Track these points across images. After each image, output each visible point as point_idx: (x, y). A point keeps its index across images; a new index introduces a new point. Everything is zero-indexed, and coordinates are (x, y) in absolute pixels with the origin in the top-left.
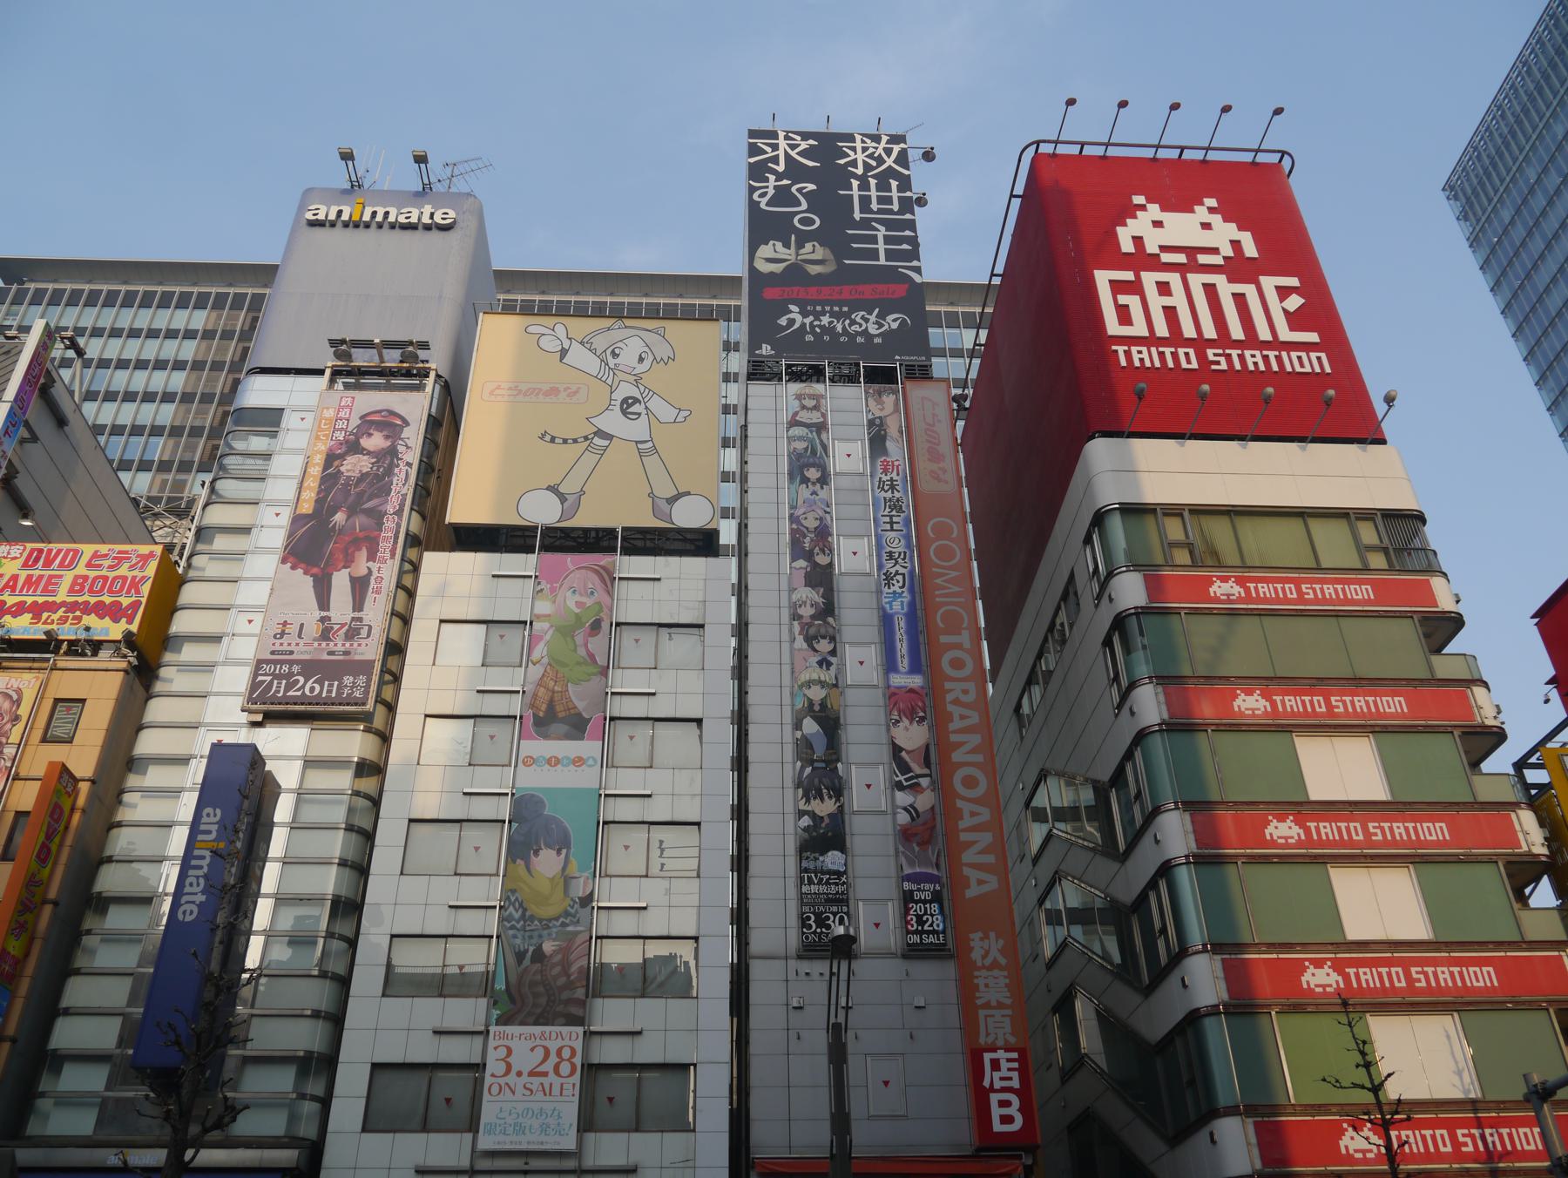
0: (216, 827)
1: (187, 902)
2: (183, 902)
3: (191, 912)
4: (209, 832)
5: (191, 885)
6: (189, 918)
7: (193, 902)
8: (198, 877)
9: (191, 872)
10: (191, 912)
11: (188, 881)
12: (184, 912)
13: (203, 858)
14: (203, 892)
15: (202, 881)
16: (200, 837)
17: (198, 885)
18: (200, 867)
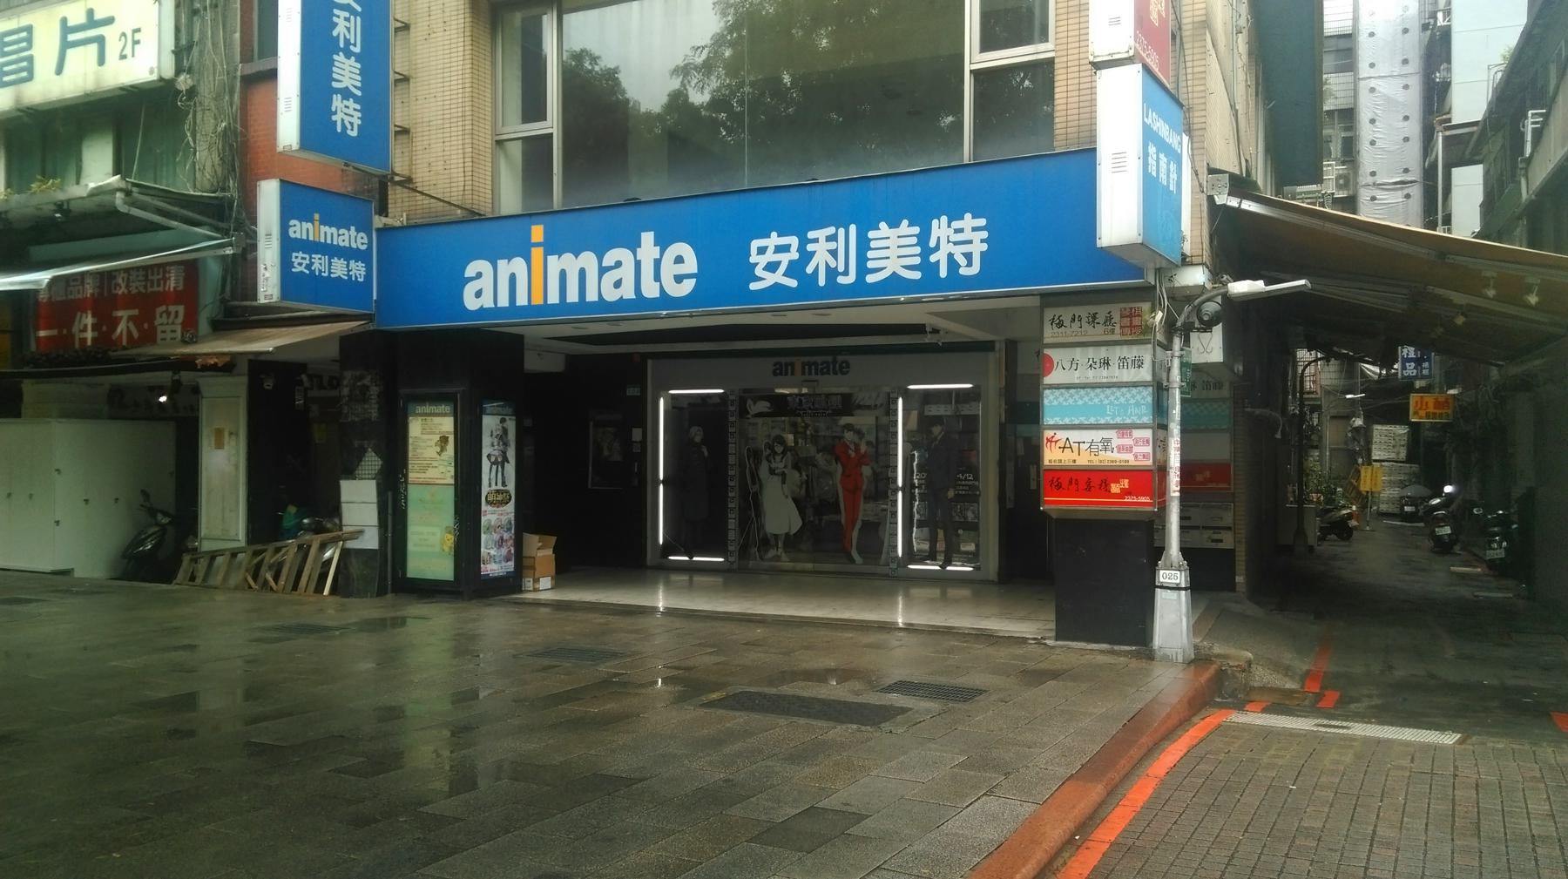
0: (502, 263)
1: (657, 278)
4: (513, 278)
5: (618, 284)
6: (691, 265)
7: (658, 263)
8: (603, 271)
9: (592, 296)
10: (679, 260)
11: (611, 295)
12: (679, 279)
13: (563, 274)
14: (634, 245)
15: (609, 259)
16: (522, 300)
17: (618, 264)
18: (582, 273)
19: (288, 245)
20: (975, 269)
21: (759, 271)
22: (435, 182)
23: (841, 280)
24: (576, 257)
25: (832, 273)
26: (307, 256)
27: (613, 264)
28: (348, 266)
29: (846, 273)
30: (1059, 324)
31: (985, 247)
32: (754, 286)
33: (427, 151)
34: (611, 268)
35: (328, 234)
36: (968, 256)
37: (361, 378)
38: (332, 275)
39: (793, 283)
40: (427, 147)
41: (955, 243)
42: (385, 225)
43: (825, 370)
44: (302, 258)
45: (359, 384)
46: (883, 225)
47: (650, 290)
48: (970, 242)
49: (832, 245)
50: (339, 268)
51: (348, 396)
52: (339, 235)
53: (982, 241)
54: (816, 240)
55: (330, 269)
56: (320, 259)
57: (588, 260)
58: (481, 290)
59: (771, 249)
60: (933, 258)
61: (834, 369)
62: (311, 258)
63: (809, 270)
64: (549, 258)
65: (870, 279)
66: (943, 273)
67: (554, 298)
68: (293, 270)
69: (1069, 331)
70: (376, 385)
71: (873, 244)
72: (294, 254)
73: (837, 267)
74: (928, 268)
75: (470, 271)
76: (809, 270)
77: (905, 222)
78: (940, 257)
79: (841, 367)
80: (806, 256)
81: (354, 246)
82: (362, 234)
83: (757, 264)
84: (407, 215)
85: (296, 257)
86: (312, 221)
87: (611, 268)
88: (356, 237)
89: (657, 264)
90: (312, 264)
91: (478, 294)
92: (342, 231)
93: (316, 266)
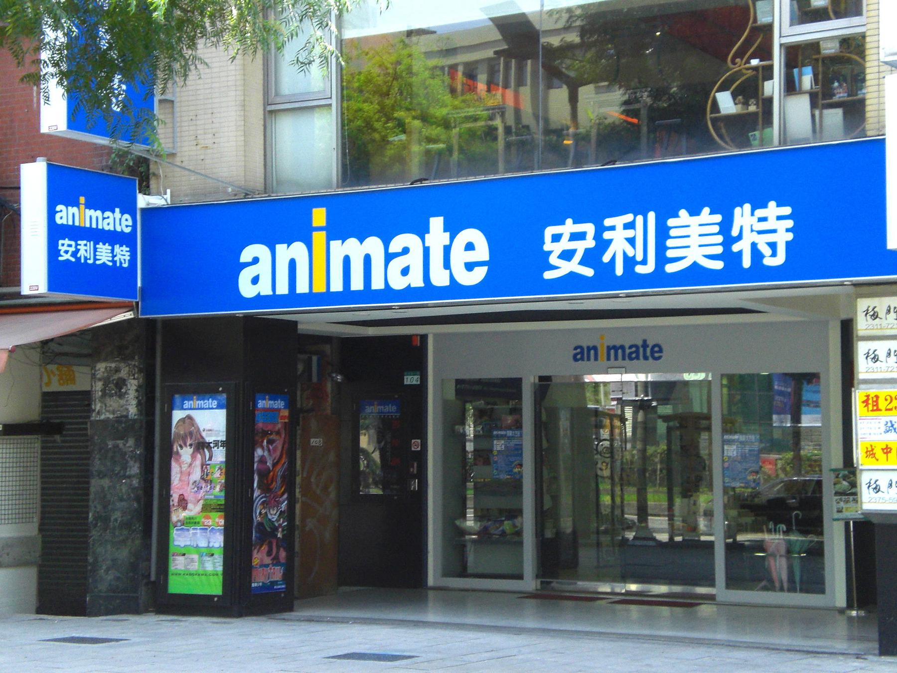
0: (281, 248)
2: (445, 282)
3: (470, 247)
4: (292, 264)
5: (405, 271)
6: (482, 252)
7: (447, 250)
8: (389, 257)
9: (377, 284)
10: (470, 247)
11: (398, 283)
12: (470, 266)
13: (347, 261)
14: (422, 231)
15: (398, 243)
16: (302, 287)
17: (406, 251)
18: (367, 260)
19: (56, 232)
20: (780, 259)
21: (553, 260)
22: (202, 157)
23: (640, 269)
24: (361, 243)
25: (629, 262)
26: (73, 243)
27: (400, 251)
28: (113, 251)
29: (644, 262)
30: (873, 315)
31: (790, 236)
32: (548, 275)
33: (194, 122)
34: (397, 255)
35: (91, 217)
36: (773, 246)
37: (117, 370)
38: (98, 262)
39: (589, 272)
40: (194, 118)
41: (760, 232)
42: (148, 204)
43: (634, 355)
44: (70, 246)
45: (116, 377)
46: (683, 213)
47: (440, 278)
48: (774, 231)
49: (630, 233)
50: (104, 254)
51: (101, 391)
52: (104, 219)
53: (788, 230)
54: (613, 228)
55: (95, 255)
56: (86, 245)
57: (374, 245)
58: (258, 275)
59: (566, 237)
60: (736, 248)
61: (645, 351)
62: (77, 245)
63: (606, 258)
64: (332, 243)
65: (670, 268)
66: (747, 263)
67: (337, 286)
68: (60, 258)
69: (884, 323)
70: (134, 379)
71: (672, 233)
72: (61, 242)
73: (635, 256)
74: (730, 258)
75: (246, 255)
76: (606, 258)
77: (706, 210)
78: (743, 246)
79: (652, 352)
80: (603, 245)
81: (118, 229)
82: (127, 216)
83: (551, 252)
84: (171, 192)
85: (63, 245)
86: (77, 204)
87: (397, 255)
88: (120, 220)
89: (447, 250)
90: (77, 251)
91: (255, 280)
92: (107, 214)
93: (82, 253)
